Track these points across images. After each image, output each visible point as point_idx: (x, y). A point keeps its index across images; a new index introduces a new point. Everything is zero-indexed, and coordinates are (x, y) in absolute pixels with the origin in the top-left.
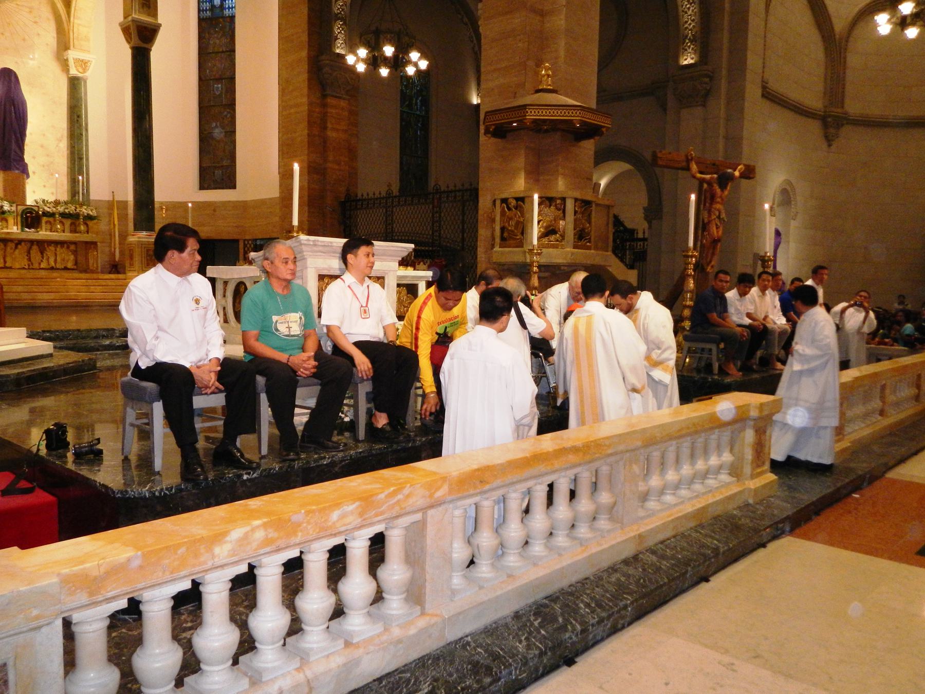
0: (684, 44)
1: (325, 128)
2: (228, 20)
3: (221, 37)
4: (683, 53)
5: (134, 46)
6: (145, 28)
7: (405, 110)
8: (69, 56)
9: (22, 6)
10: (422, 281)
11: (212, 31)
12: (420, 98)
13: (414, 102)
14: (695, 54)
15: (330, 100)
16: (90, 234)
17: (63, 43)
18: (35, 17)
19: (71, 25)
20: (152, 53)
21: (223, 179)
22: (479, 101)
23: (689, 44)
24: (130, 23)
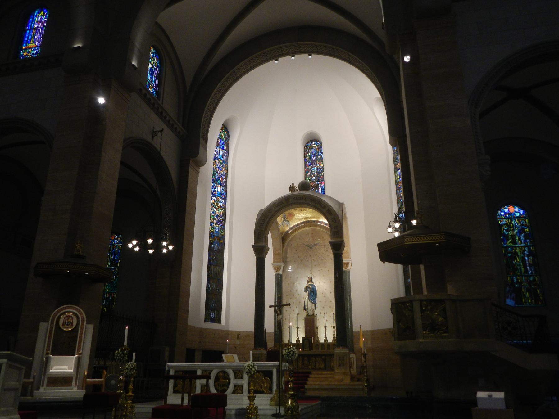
9: (321, 245)
10: (274, 368)
12: (523, 234)
13: (517, 238)
18: (326, 249)
20: (343, 255)
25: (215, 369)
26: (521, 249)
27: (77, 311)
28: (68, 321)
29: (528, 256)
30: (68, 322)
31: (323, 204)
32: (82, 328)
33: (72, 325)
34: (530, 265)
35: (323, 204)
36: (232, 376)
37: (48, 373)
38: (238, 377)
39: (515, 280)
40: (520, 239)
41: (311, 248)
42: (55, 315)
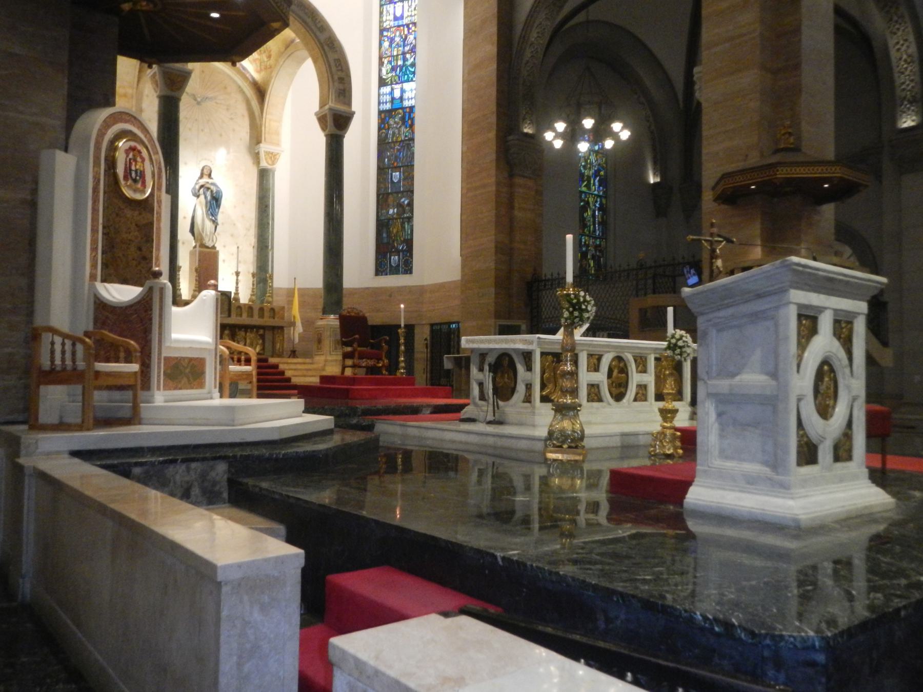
0: (901, 106)
1: (511, 207)
2: (408, 110)
3: (400, 127)
4: (901, 115)
5: (330, 133)
6: (340, 116)
7: (584, 189)
8: (260, 150)
9: (221, 104)
11: (391, 122)
12: (598, 178)
14: (917, 113)
15: (518, 181)
16: (276, 319)
17: (256, 137)
19: (264, 119)
21: (398, 265)
22: (658, 180)
23: (908, 106)
24: (327, 112)
25: (609, 352)
26: (594, 198)
27: (146, 136)
28: (135, 166)
29: (599, 210)
30: (136, 171)
31: (319, 22)
32: (159, 202)
33: (144, 184)
34: (599, 223)
35: (319, 22)
36: (632, 366)
37: (167, 344)
38: (640, 369)
39: (583, 240)
40: (594, 184)
41: (199, 103)
42: (101, 134)
